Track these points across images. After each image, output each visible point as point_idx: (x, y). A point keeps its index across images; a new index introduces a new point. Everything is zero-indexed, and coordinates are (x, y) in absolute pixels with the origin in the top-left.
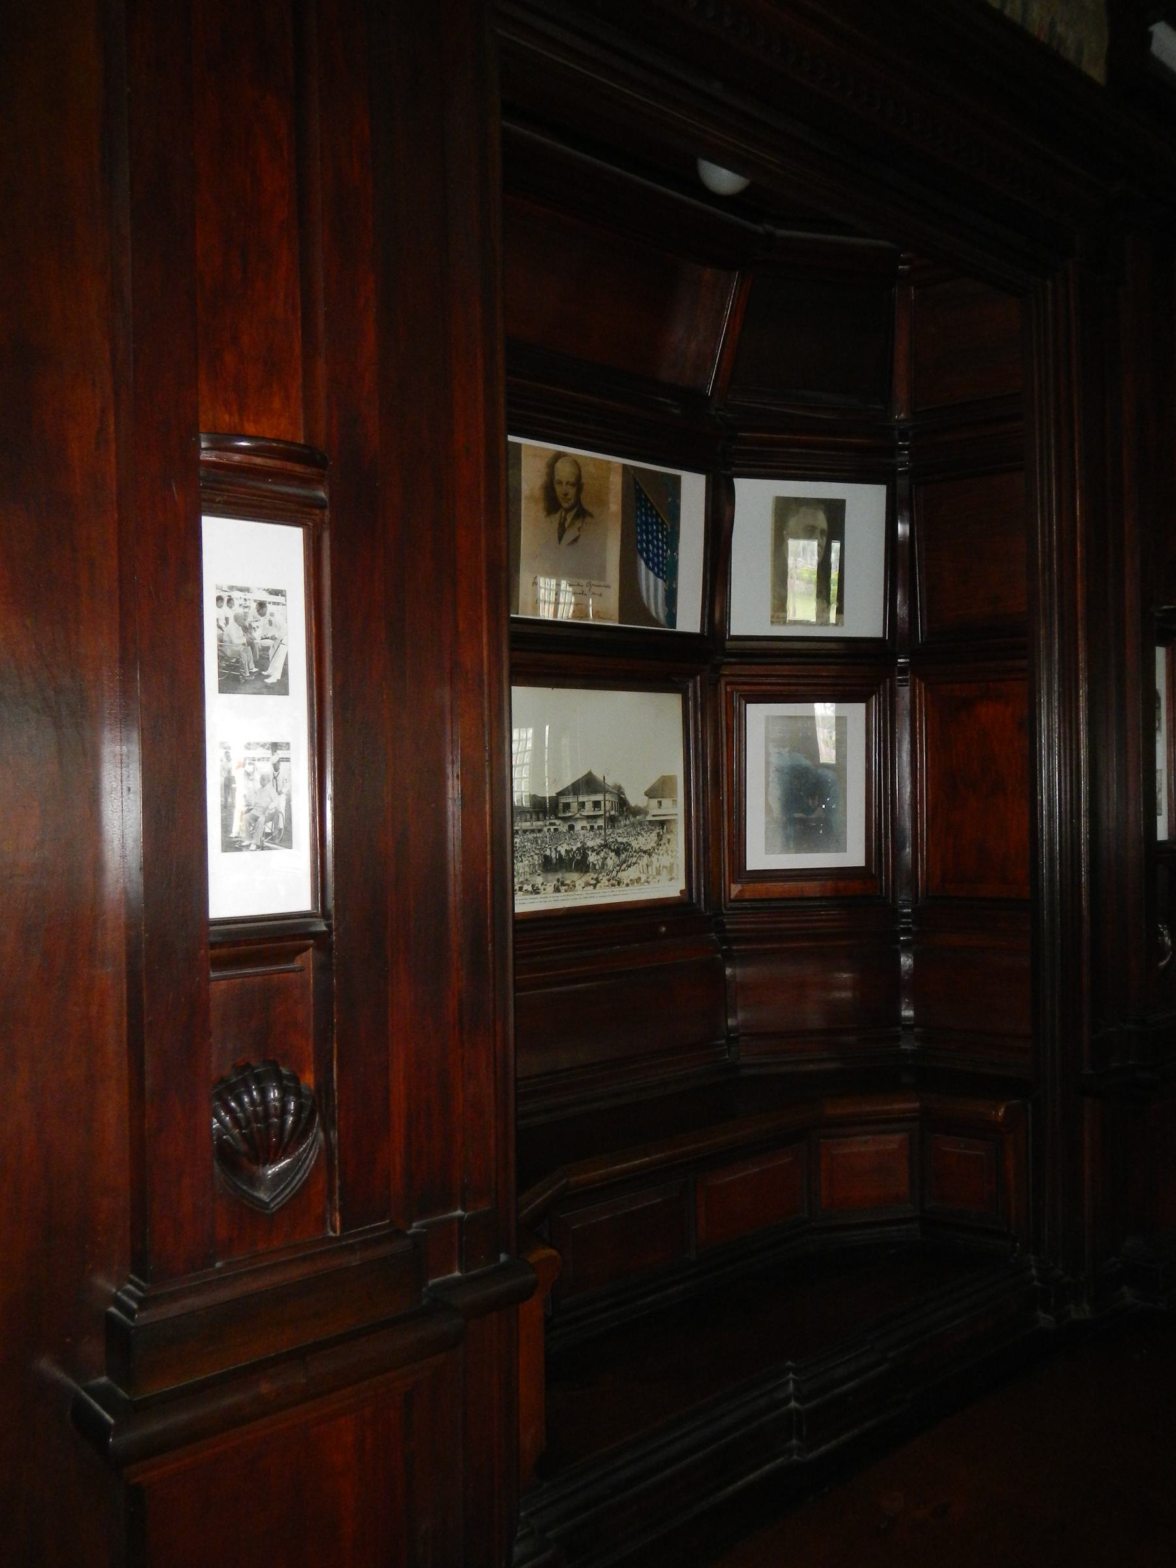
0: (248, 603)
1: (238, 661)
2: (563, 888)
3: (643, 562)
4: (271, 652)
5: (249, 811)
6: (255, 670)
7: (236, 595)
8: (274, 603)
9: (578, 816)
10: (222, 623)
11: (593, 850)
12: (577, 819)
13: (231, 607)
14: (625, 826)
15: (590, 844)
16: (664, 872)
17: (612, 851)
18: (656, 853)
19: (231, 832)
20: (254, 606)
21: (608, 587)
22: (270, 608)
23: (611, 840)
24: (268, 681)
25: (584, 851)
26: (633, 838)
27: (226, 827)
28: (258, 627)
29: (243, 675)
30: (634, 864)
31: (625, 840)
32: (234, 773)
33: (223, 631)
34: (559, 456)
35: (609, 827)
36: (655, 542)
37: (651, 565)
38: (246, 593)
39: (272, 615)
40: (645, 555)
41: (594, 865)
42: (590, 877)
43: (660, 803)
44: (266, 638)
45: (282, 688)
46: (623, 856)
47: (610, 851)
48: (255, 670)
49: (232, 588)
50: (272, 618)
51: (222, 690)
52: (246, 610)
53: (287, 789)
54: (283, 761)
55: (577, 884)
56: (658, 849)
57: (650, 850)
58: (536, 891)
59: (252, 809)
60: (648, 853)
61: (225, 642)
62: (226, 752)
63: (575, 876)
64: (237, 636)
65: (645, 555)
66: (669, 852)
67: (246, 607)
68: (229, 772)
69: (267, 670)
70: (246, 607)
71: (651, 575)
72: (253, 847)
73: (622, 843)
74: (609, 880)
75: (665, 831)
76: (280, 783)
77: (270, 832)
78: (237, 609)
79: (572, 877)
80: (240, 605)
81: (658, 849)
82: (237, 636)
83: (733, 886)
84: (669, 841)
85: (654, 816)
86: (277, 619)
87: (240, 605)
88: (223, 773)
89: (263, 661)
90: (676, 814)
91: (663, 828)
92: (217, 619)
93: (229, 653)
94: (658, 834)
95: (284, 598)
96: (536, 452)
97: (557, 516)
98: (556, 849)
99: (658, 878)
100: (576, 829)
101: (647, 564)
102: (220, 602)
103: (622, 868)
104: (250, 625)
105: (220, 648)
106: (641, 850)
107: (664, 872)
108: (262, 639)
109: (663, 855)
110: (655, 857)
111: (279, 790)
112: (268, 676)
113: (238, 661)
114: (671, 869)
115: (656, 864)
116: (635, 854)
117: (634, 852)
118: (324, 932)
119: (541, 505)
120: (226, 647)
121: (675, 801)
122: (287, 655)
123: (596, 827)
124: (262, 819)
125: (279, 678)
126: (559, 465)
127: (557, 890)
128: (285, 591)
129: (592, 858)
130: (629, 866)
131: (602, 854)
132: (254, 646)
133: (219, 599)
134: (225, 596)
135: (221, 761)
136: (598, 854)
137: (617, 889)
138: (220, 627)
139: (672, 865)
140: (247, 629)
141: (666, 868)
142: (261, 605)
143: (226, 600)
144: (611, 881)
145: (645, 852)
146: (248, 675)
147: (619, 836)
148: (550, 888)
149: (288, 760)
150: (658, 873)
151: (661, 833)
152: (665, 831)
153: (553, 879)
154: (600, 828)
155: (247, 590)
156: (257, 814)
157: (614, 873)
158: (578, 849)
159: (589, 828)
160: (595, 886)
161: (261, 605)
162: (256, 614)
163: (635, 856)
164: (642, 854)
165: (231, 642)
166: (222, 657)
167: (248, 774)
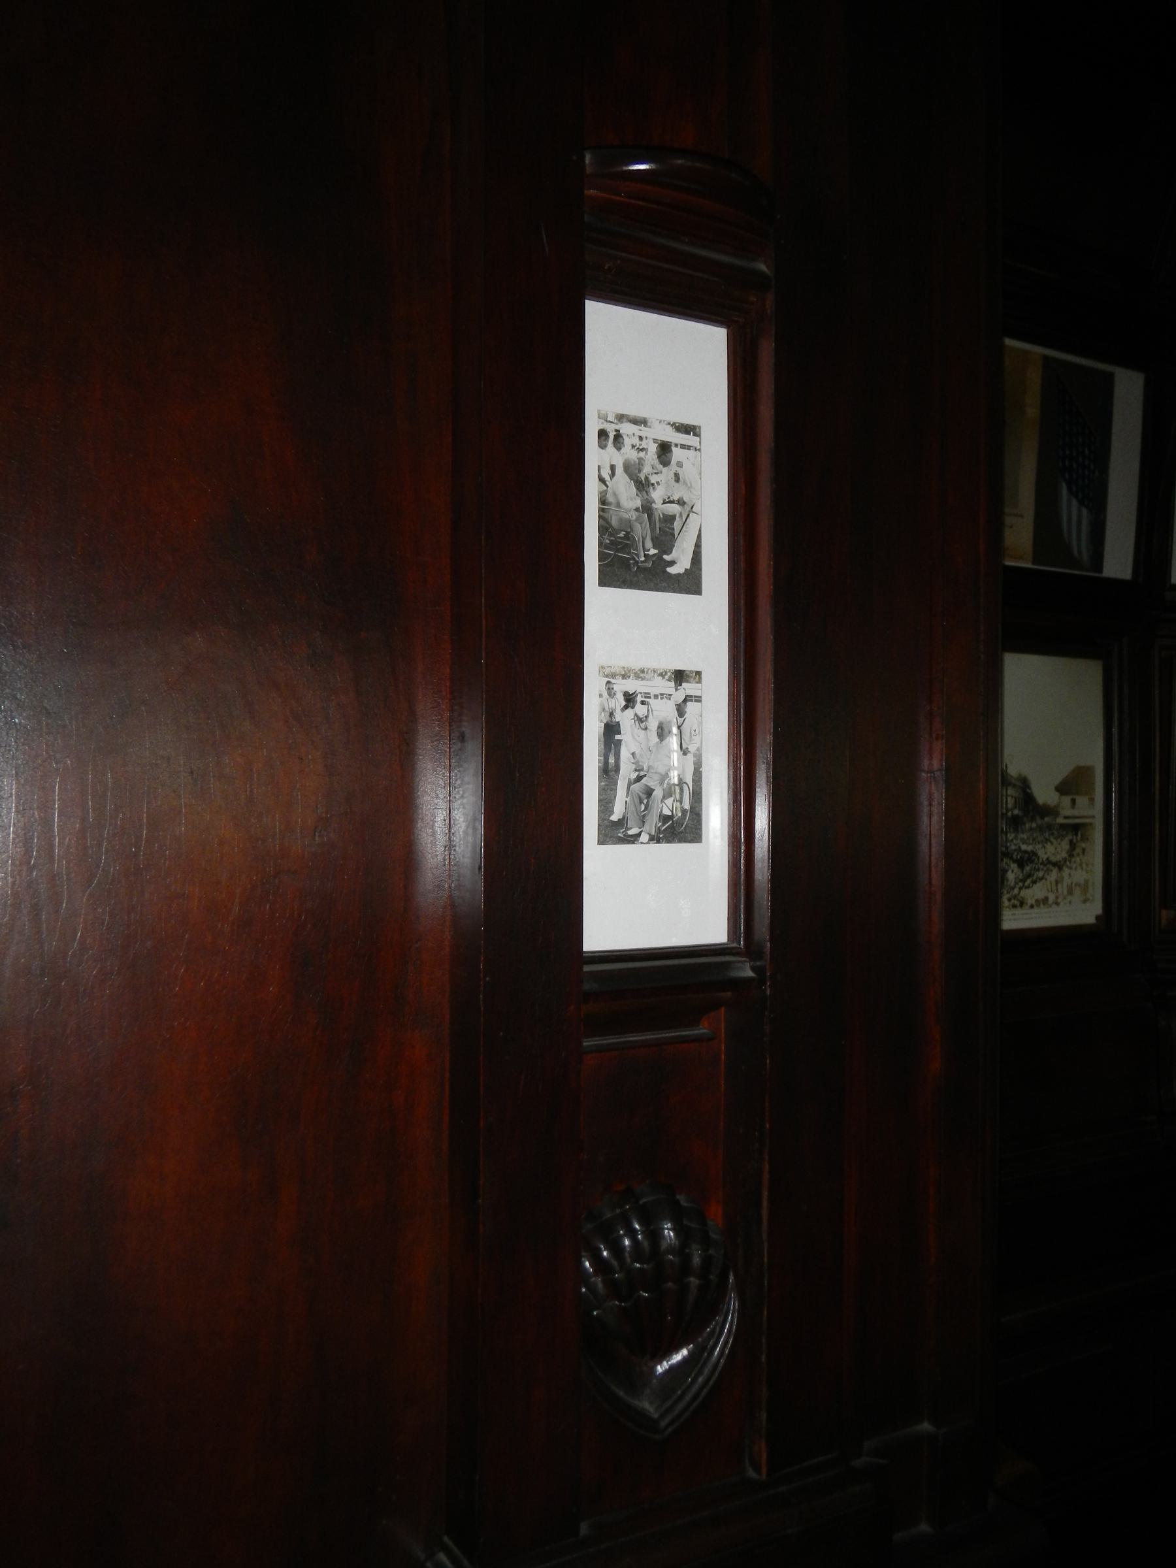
0: (644, 445)
1: (627, 536)
3: (1064, 485)
4: (677, 525)
5: (639, 779)
6: (653, 552)
7: (626, 429)
8: (683, 447)
10: (606, 474)
13: (619, 449)
14: (1031, 829)
16: (1077, 891)
17: (1014, 861)
18: (1067, 867)
19: (612, 812)
20: (653, 448)
21: (1022, 516)
22: (677, 454)
23: (1013, 847)
24: (672, 570)
26: (1040, 846)
27: (605, 804)
28: (658, 483)
29: (634, 559)
30: (1041, 879)
31: (1030, 848)
32: (618, 717)
33: (607, 486)
35: (1012, 830)
36: (1080, 459)
37: (1074, 489)
38: (642, 427)
39: (680, 465)
40: (1067, 476)
43: (1073, 801)
44: (672, 502)
45: (690, 583)
46: (1027, 869)
47: (1011, 862)
48: (653, 552)
49: (621, 418)
50: (679, 471)
51: (602, 583)
52: (642, 454)
53: (698, 745)
54: (692, 701)
56: (1070, 862)
57: (1060, 862)
59: (645, 776)
60: (1059, 866)
61: (609, 504)
62: (608, 682)
64: (627, 497)
65: (1067, 476)
66: (1084, 865)
67: (642, 450)
68: (611, 714)
69: (671, 552)
70: (642, 450)
71: (1074, 502)
72: (644, 837)
73: (1026, 852)
74: (1009, 900)
75: (1079, 838)
76: (686, 737)
77: (670, 814)
80: (633, 446)
81: (1070, 862)
82: (627, 497)
83: (1164, 912)
84: (1084, 850)
85: (1066, 818)
86: (687, 472)
87: (633, 446)
88: (603, 714)
89: (665, 536)
90: (1093, 817)
91: (1076, 835)
92: (599, 466)
93: (614, 522)
94: (1071, 842)
95: (698, 438)
99: (1069, 898)
101: (1070, 489)
102: (603, 438)
103: (1026, 884)
104: (647, 478)
105: (602, 513)
106: (1049, 861)
107: (1077, 891)
108: (664, 502)
109: (1076, 869)
110: (1066, 871)
111: (684, 747)
112: (672, 563)
113: (627, 536)
114: (1085, 887)
115: (1067, 881)
116: (1042, 867)
117: (1041, 864)
118: (749, 980)
120: (611, 512)
121: (1092, 800)
122: (700, 531)
124: (658, 793)
125: (688, 567)
128: (700, 427)
130: (1034, 882)
132: (652, 514)
133: (602, 434)
134: (611, 429)
135: (601, 696)
137: (1019, 911)
138: (602, 480)
139: (1086, 882)
140: (643, 486)
141: (1079, 886)
142: (664, 449)
143: (612, 436)
144: (1013, 901)
145: (1054, 864)
146: (643, 559)
147: (1023, 843)
149: (698, 699)
150: (1070, 892)
151: (1075, 841)
152: (1079, 838)
155: (641, 422)
156: (652, 784)
157: (1016, 891)
161: (664, 449)
162: (656, 462)
163: (1042, 870)
164: (1051, 867)
165: (618, 505)
166: (604, 528)
167: (640, 720)
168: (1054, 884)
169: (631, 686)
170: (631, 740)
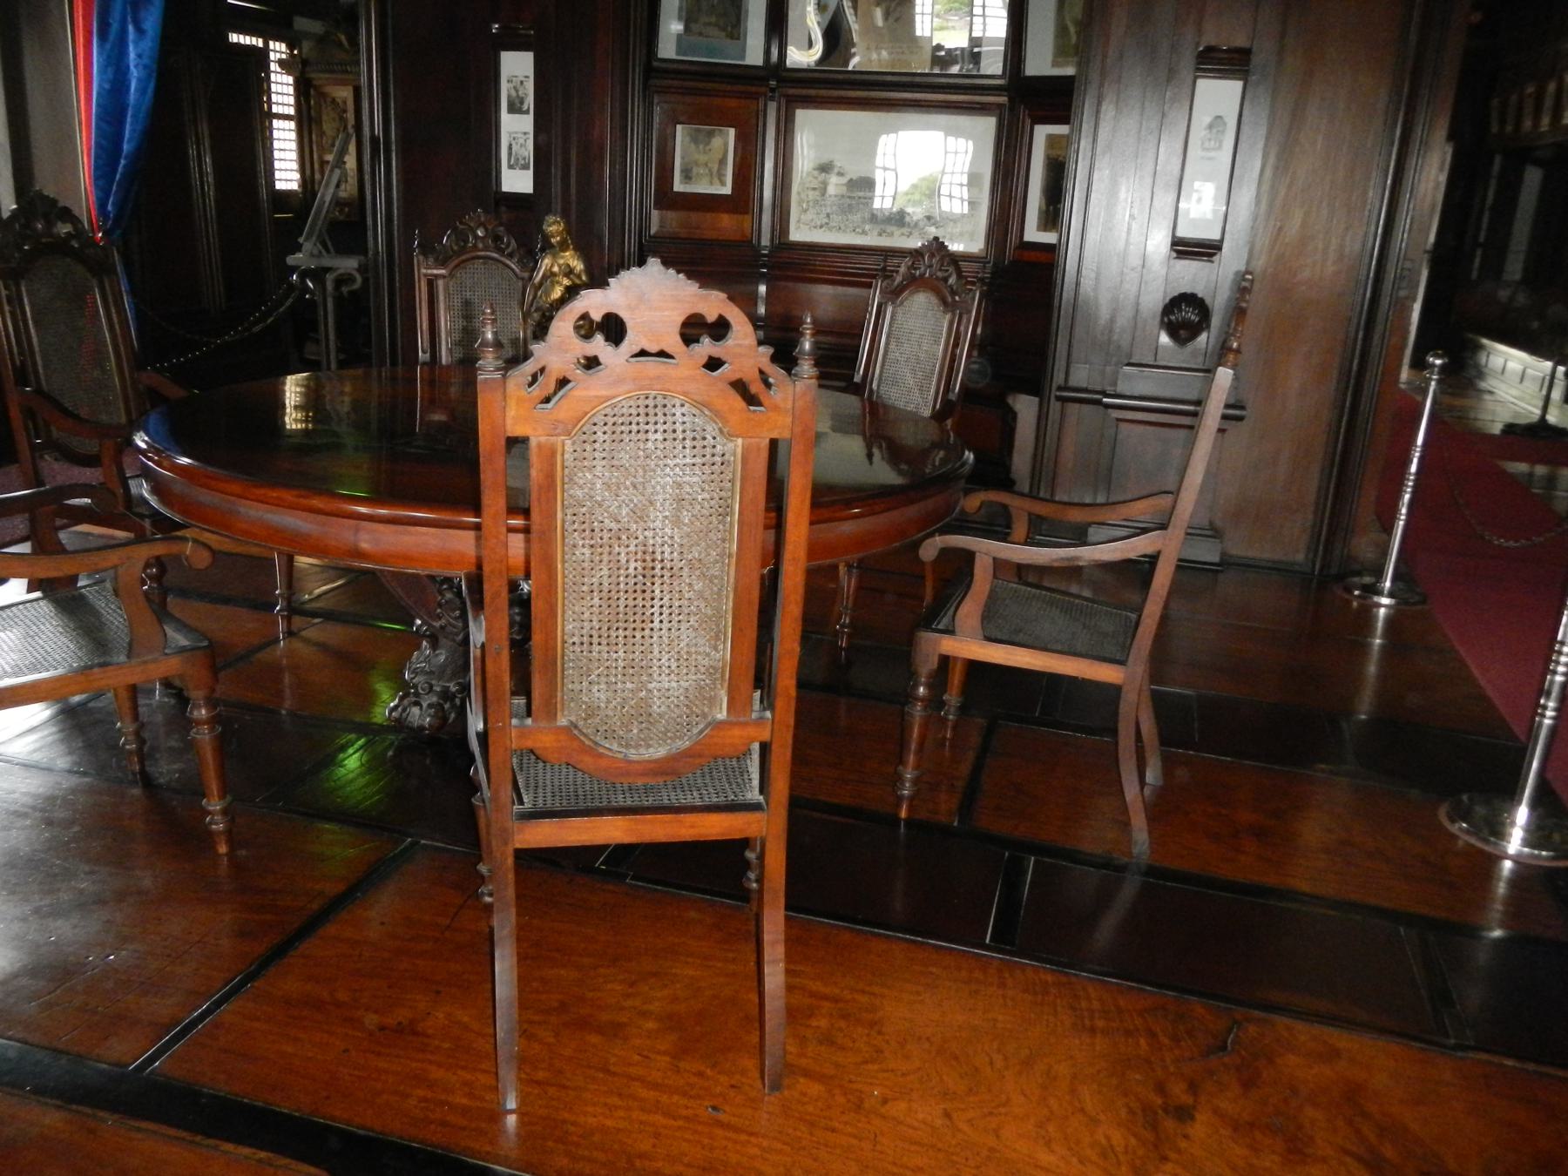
42: (905, 230)
45: (527, 112)
58: (864, 233)
63: (894, 229)
64: (514, 93)
78: (514, 84)
79: (890, 229)
82: (514, 93)
89: (522, 102)
110: (959, 225)
121: (981, 190)
127: (880, 235)
140: (517, 91)
160: (908, 236)
161: (522, 82)
170: (515, 148)
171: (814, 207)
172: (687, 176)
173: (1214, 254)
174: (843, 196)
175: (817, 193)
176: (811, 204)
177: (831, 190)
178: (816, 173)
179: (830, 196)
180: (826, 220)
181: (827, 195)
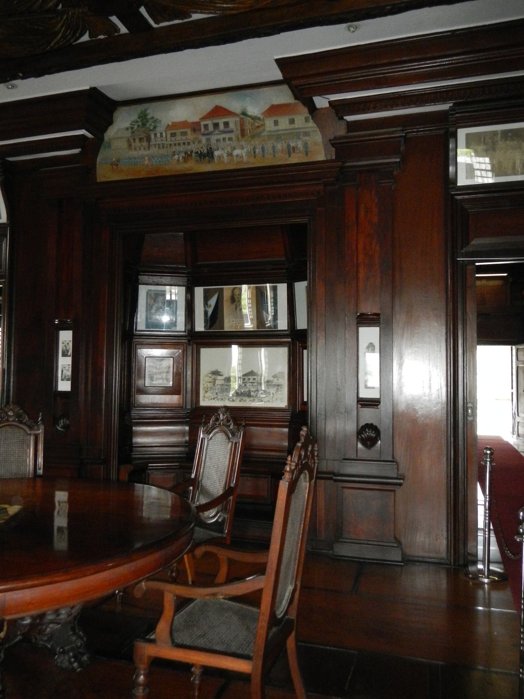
2: (242, 401)
9: (248, 382)
11: (253, 391)
12: (247, 383)
15: (252, 390)
22: (69, 344)
25: (249, 391)
27: (62, 377)
34: (235, 288)
41: (253, 396)
42: (252, 399)
55: (247, 400)
58: (233, 401)
63: (246, 398)
64: (64, 348)
74: (258, 400)
78: (65, 344)
79: (244, 398)
82: (64, 348)
84: (281, 391)
94: (277, 388)
96: (227, 289)
97: (234, 304)
98: (240, 390)
100: (247, 385)
114: (282, 399)
119: (230, 302)
121: (284, 379)
123: (254, 385)
126: (235, 291)
127: (240, 401)
129: (252, 394)
131: (256, 393)
136: (254, 392)
140: (66, 347)
148: (238, 400)
150: (277, 399)
153: (239, 398)
154: (255, 385)
155: (66, 341)
158: (248, 391)
159: (251, 385)
160: (253, 401)
161: (68, 343)
168: (272, 398)
169: (64, 366)
170: (64, 372)
171: (210, 390)
172: (152, 379)
173: (379, 405)
174: (223, 385)
175: (212, 384)
176: (209, 389)
177: (217, 382)
178: (210, 375)
179: (217, 385)
180: (216, 396)
181: (216, 385)
